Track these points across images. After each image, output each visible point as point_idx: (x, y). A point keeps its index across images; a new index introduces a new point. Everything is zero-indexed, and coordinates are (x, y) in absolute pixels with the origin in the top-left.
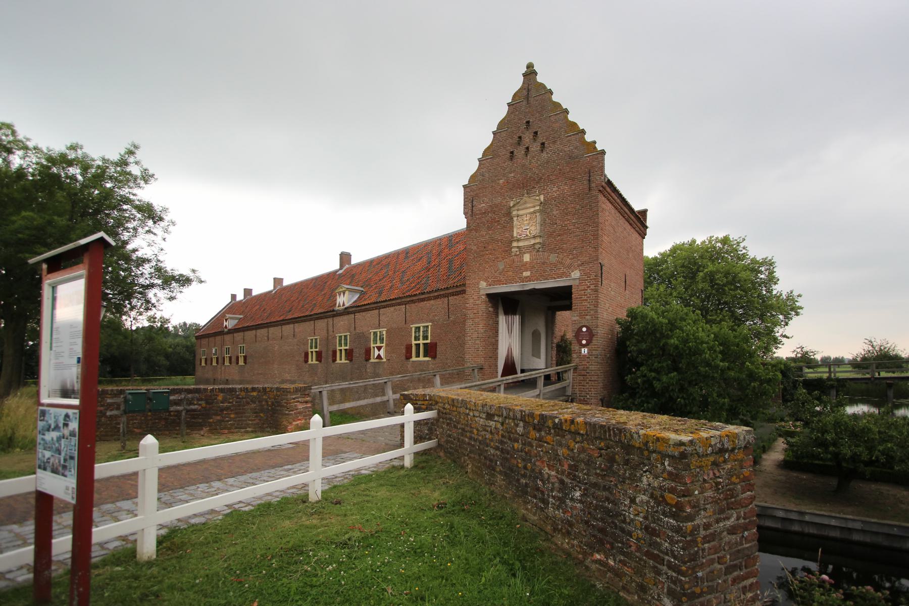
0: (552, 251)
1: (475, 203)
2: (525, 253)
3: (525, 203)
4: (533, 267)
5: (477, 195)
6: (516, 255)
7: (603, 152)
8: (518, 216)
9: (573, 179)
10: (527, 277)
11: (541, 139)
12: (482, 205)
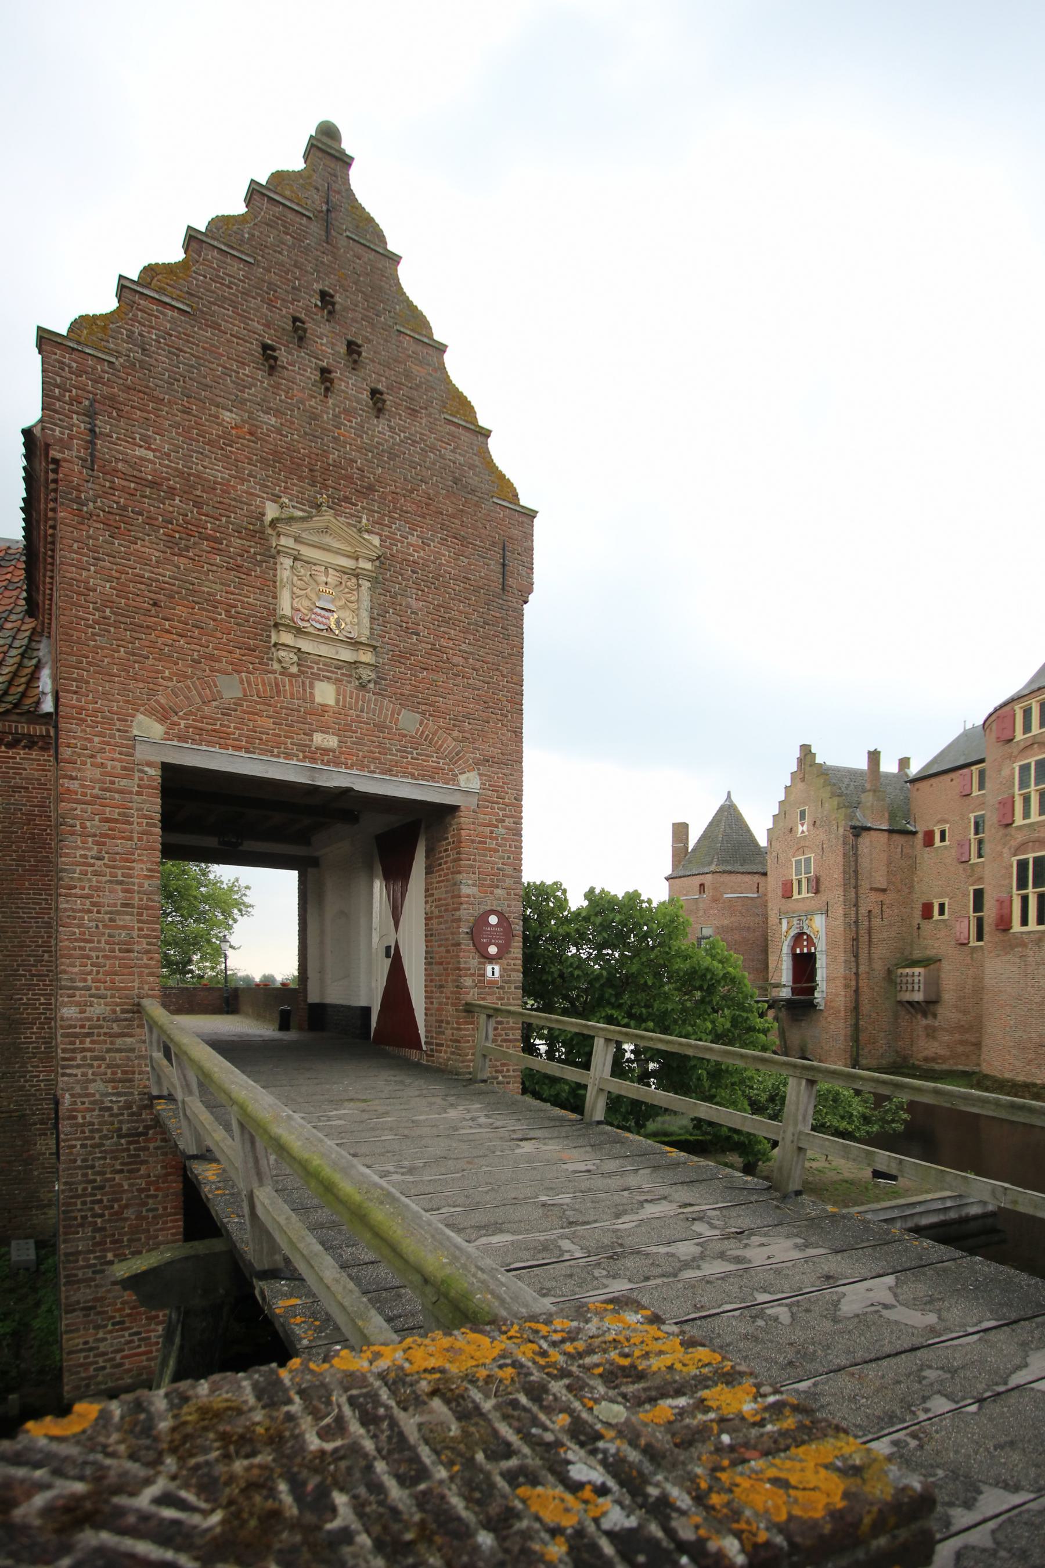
0: (405, 701)
2: (317, 677)
3: (326, 530)
6: (284, 672)
8: (295, 559)
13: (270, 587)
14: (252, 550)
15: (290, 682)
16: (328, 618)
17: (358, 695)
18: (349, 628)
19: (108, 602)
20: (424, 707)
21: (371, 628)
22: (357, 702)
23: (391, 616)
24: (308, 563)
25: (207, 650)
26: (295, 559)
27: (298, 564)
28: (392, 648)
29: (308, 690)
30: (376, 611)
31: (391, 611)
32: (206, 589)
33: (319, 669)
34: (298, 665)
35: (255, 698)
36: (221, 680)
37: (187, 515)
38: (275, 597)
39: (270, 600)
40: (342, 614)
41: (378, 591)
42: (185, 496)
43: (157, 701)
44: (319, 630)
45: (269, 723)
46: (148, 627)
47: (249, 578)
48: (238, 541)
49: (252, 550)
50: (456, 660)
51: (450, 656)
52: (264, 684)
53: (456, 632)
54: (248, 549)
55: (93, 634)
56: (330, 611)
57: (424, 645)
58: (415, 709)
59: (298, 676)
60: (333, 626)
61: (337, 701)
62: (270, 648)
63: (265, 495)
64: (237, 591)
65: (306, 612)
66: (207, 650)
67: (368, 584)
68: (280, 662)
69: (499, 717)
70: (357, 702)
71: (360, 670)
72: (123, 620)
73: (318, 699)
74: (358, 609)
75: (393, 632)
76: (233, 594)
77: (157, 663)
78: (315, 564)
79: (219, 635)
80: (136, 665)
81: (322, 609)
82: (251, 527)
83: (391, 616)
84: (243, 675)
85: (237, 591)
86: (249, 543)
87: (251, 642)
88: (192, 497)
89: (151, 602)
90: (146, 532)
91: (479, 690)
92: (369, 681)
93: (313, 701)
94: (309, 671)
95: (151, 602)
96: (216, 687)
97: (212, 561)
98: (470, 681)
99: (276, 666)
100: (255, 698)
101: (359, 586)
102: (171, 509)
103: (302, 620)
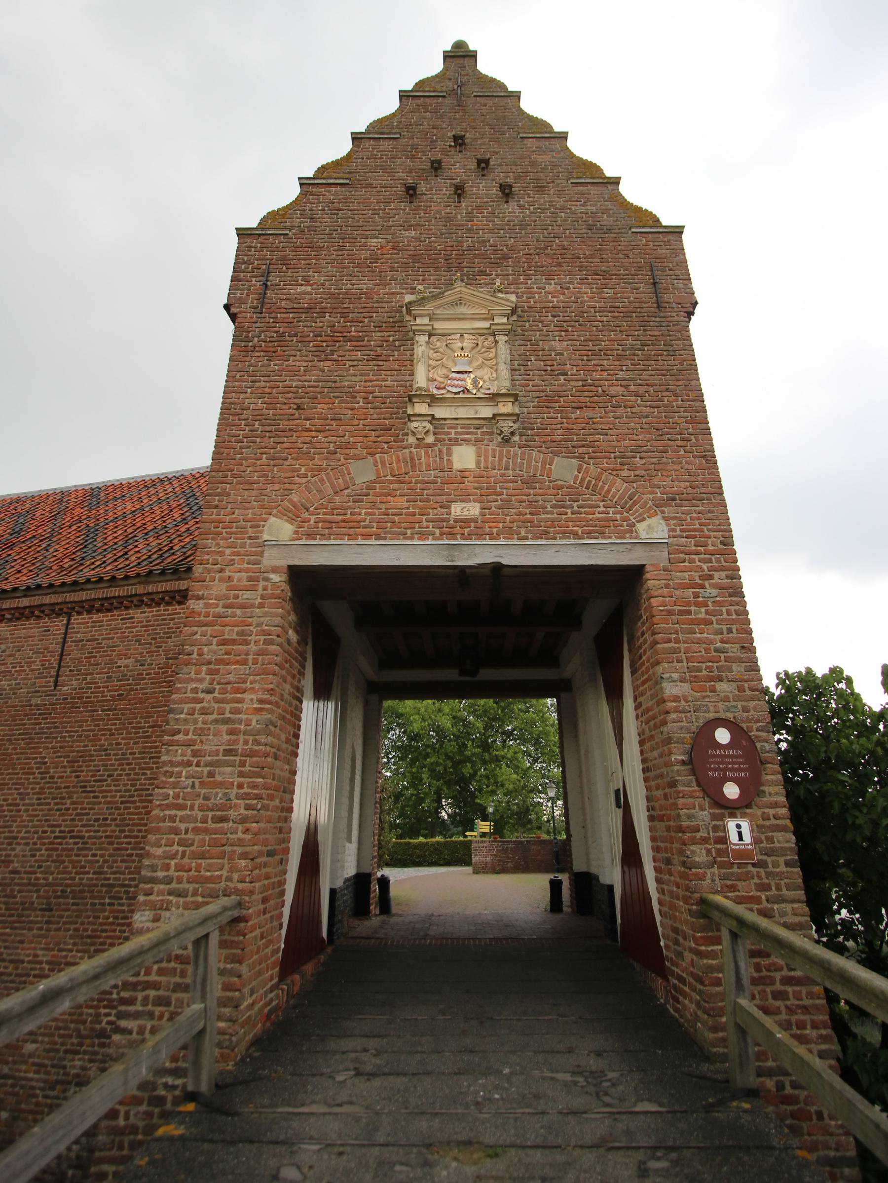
0: (556, 448)
1: (273, 279)
2: (455, 442)
3: (459, 302)
4: (492, 491)
5: (284, 260)
6: (420, 444)
7: (678, 231)
9: (605, 275)
10: (466, 522)
11: (499, 175)
12: (299, 289)
13: (408, 366)
14: (391, 339)
15: (426, 453)
16: (464, 380)
17: (501, 452)
18: (486, 385)
19: (259, 417)
20: (581, 450)
21: (512, 380)
22: (500, 460)
23: (534, 363)
24: (443, 335)
25: (343, 439)
26: (431, 335)
27: (434, 339)
28: (537, 394)
29: (445, 458)
30: (516, 363)
31: (533, 358)
32: (346, 383)
33: (457, 433)
34: (435, 434)
35: (389, 478)
36: (354, 466)
37: (334, 326)
38: (412, 374)
39: (407, 378)
40: (479, 373)
41: (517, 343)
42: (335, 311)
43: (291, 501)
44: (456, 393)
45: (402, 502)
46: (290, 430)
47: (388, 363)
48: (379, 334)
49: (391, 339)
50: (613, 391)
51: (605, 388)
52: (398, 461)
53: (610, 362)
54: (387, 338)
55: (241, 448)
56: (466, 372)
57: (573, 383)
58: (570, 455)
59: (434, 445)
60: (470, 386)
61: (478, 463)
62: (405, 423)
63: (404, 291)
64: (375, 378)
65: (441, 380)
66: (343, 439)
67: (506, 338)
68: (414, 434)
69: (679, 443)
70: (500, 460)
71: (501, 424)
72: (268, 428)
73: (457, 465)
74: (497, 364)
75: (537, 378)
76: (371, 381)
77: (294, 462)
78: (450, 334)
79: (356, 422)
80: (275, 469)
81: (458, 372)
82: (391, 320)
83: (534, 363)
84: (377, 456)
85: (375, 378)
86: (388, 334)
87: (387, 422)
88: (340, 310)
89: (295, 407)
90: (298, 348)
91: (647, 417)
92: (512, 434)
93: (450, 469)
94: (446, 437)
95: (295, 407)
96: (349, 474)
97: (353, 358)
98: (634, 410)
99: (411, 440)
100: (389, 478)
101: (496, 342)
102: (321, 324)
103: (438, 388)
